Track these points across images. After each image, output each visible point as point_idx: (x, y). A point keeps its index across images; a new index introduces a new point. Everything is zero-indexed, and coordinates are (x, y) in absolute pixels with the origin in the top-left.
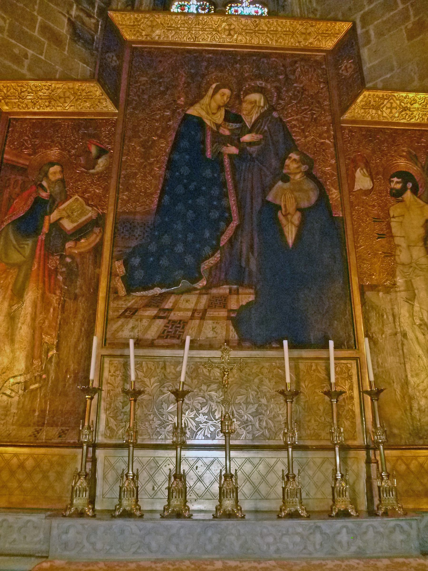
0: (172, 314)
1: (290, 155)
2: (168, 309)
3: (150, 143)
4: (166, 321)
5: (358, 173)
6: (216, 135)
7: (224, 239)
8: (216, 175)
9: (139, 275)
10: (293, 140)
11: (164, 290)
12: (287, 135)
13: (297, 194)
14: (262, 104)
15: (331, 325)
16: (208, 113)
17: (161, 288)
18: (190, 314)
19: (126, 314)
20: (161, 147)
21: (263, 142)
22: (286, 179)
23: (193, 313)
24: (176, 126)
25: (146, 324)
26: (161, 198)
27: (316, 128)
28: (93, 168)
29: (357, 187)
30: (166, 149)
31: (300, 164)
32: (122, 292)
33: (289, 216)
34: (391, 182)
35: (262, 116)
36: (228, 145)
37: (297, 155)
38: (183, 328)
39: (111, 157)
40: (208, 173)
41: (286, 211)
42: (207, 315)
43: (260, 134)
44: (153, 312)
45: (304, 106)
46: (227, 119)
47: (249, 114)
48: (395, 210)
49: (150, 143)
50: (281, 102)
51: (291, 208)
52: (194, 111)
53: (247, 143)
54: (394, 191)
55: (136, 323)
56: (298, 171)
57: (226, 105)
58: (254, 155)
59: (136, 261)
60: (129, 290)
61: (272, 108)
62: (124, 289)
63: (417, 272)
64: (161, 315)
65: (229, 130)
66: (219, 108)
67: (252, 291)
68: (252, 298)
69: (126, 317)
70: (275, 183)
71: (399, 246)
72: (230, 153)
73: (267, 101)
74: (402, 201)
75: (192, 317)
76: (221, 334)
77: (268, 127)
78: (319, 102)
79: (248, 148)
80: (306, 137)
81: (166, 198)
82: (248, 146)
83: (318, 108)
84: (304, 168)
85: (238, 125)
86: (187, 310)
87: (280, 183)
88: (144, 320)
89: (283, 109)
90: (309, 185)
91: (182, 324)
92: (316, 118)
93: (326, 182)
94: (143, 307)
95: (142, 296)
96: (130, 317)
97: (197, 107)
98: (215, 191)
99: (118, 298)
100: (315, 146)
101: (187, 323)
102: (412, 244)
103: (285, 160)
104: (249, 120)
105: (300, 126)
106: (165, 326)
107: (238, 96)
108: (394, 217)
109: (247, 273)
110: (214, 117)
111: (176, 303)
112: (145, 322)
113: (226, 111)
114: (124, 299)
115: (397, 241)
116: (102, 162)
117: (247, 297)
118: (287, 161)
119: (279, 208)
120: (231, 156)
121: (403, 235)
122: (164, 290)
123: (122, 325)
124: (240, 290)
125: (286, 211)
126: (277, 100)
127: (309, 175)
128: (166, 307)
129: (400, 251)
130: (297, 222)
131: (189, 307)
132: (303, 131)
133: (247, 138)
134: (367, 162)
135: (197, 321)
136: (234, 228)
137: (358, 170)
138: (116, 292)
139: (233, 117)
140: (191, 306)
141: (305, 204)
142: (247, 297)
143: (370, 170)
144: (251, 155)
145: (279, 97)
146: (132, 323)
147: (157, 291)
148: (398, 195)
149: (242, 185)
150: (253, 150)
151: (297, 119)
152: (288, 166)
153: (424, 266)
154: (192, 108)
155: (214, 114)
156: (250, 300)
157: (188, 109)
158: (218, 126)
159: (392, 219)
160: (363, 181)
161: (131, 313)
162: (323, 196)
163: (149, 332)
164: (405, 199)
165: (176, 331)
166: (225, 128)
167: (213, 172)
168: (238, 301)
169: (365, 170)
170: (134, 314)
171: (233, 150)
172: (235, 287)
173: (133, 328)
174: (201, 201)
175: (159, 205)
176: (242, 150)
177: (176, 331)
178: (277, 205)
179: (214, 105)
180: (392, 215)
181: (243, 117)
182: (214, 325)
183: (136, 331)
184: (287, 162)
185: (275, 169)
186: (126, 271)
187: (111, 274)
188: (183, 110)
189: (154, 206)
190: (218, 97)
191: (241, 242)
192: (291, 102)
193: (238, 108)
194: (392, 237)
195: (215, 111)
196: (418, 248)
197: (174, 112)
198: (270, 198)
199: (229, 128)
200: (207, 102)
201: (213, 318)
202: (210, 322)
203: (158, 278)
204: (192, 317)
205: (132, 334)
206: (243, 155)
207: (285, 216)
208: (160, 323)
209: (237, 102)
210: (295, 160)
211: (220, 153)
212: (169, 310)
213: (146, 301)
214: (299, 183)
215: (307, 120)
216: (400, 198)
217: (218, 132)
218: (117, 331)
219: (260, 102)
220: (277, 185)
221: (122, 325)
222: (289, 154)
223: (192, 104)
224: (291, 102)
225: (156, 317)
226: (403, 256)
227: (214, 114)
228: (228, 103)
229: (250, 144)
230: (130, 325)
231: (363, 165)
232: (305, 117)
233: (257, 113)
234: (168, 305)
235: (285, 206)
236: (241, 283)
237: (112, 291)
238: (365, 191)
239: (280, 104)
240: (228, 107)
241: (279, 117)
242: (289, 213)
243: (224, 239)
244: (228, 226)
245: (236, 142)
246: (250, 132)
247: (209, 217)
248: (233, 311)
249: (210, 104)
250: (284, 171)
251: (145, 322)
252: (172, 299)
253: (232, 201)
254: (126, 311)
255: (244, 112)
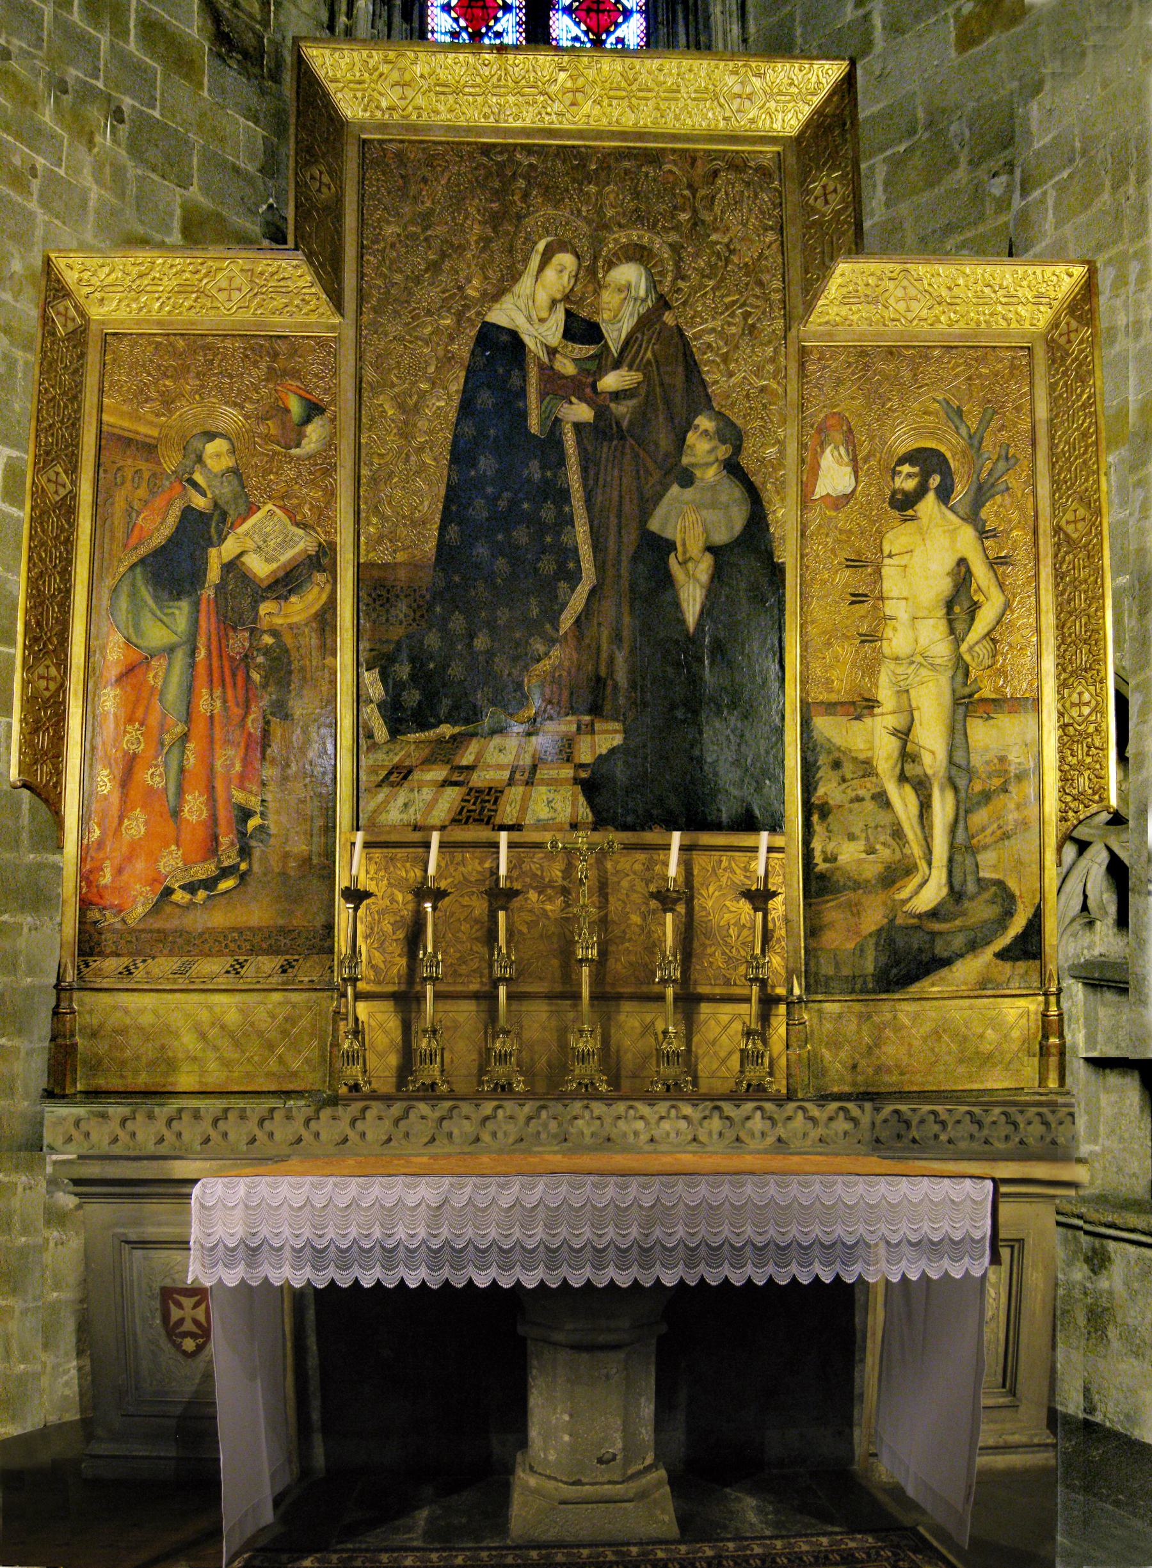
0: (475, 776)
1: (696, 422)
2: (467, 768)
3: (415, 397)
4: (464, 790)
5: (828, 459)
6: (549, 374)
7: (567, 620)
8: (549, 474)
9: (412, 697)
10: (703, 383)
11: (457, 730)
12: (692, 368)
13: (704, 513)
14: (642, 293)
15: (759, 789)
16: (529, 319)
17: (454, 724)
18: (506, 774)
19: (392, 778)
20: (438, 408)
21: (643, 392)
22: (687, 479)
23: (513, 773)
24: (466, 355)
25: (430, 797)
26: (442, 529)
27: (753, 351)
28: (298, 445)
29: (823, 488)
30: (447, 414)
31: (715, 442)
32: (381, 733)
33: (690, 565)
34: (894, 473)
35: (644, 323)
36: (573, 399)
37: (711, 420)
38: (495, 802)
39: (333, 420)
40: (534, 469)
41: (684, 553)
42: (538, 776)
43: (638, 370)
44: (439, 773)
45: (728, 295)
46: (569, 334)
47: (616, 319)
48: (897, 538)
49: (415, 397)
50: (681, 284)
51: (695, 547)
52: (504, 314)
53: (611, 393)
54: (899, 497)
55: (411, 795)
56: (712, 458)
57: (567, 298)
58: (625, 424)
59: (403, 671)
60: (395, 732)
61: (663, 304)
62: (384, 729)
63: (924, 672)
64: (455, 778)
65: (574, 360)
66: (554, 303)
67: (617, 726)
68: (618, 740)
69: (392, 785)
70: (666, 488)
71: (892, 618)
72: (575, 420)
73: (653, 284)
74: (913, 519)
75: (511, 782)
76: (564, 812)
77: (653, 352)
78: (760, 284)
79: (613, 405)
80: (731, 374)
81: (453, 530)
82: (611, 400)
83: (757, 297)
84: (724, 451)
85: (592, 350)
86: (500, 767)
87: (675, 489)
88: (425, 790)
89: (684, 303)
90: (732, 492)
91: (494, 794)
92: (753, 325)
93: (764, 484)
94: (423, 763)
95: (418, 743)
96: (399, 784)
97: (507, 302)
98: (548, 513)
99: (374, 747)
100: (747, 396)
101: (502, 792)
102: (921, 615)
103: (687, 432)
104: (616, 334)
105: (719, 349)
106: (463, 800)
107: (592, 271)
108: (890, 556)
109: (609, 690)
110: (543, 328)
111: (479, 756)
112: (427, 794)
113: (569, 314)
114: (385, 748)
115: (890, 608)
116: (315, 432)
117: (608, 738)
118: (690, 434)
119: (671, 546)
120: (578, 427)
121: (905, 594)
122: (457, 730)
123: (386, 801)
124: (597, 726)
125: (684, 553)
126: (675, 279)
127: (733, 468)
128: (464, 762)
129: (895, 629)
130: (704, 577)
131: (506, 761)
132: (725, 359)
133: (611, 381)
134: (850, 430)
135: (521, 789)
136: (585, 595)
137: (828, 451)
138: (370, 736)
139: (582, 329)
140: (507, 759)
141: (721, 537)
142: (608, 738)
143: (854, 451)
144: (618, 424)
145: (680, 276)
146: (402, 796)
147: (446, 730)
148: (904, 503)
149: (600, 499)
150: (622, 410)
151: (713, 330)
152: (691, 447)
153: (938, 661)
154: (497, 306)
155: (542, 321)
156: (615, 743)
157: (490, 309)
158: (552, 352)
159: (887, 561)
160: (835, 475)
161: (400, 775)
162: (757, 519)
163: (434, 813)
164: (919, 514)
165: (483, 808)
166: (566, 357)
167: (543, 468)
168: (593, 747)
169: (842, 450)
170: (405, 778)
171: (583, 412)
172: (587, 718)
173: (406, 805)
174: (521, 535)
175: (441, 545)
176: (601, 413)
177: (483, 808)
178: (667, 540)
179: (543, 298)
180: (886, 553)
181: (603, 326)
182: (551, 796)
183: (412, 811)
184: (691, 437)
185: (667, 455)
186: (386, 691)
187: (359, 699)
188: (478, 314)
189: (430, 546)
190: (550, 273)
191: (599, 624)
192: (702, 286)
193: (592, 305)
194: (882, 598)
195: (544, 315)
196: (931, 621)
197: (460, 316)
198: (654, 525)
199: (574, 356)
200: (528, 292)
201: (549, 782)
202: (543, 789)
203: (445, 704)
204: (511, 782)
205: (405, 817)
206: (603, 429)
207: (683, 564)
208: (452, 795)
209: (590, 288)
210: (706, 432)
211: (557, 421)
212: (471, 768)
213: (427, 751)
214: (713, 487)
215: (733, 330)
216: (910, 512)
217: (552, 368)
218: (377, 811)
219: (638, 287)
220: (668, 494)
221: (386, 801)
222: (695, 417)
223: (497, 297)
224: (702, 286)
225: (446, 783)
226: (897, 641)
227: (542, 321)
228: (572, 290)
229: (616, 396)
230: (401, 801)
231: (838, 437)
232: (729, 324)
233: (632, 315)
234: (467, 759)
235: (684, 540)
236: (596, 710)
237: (362, 732)
238: (838, 498)
239: (679, 290)
240: (572, 302)
241: (677, 326)
242: (690, 558)
243: (567, 620)
244: (573, 590)
245: (588, 390)
246: (617, 365)
247: (536, 570)
248: (582, 766)
249: (533, 297)
250: (685, 460)
251: (427, 794)
252: (474, 746)
253: (581, 533)
254: (390, 773)
255: (606, 315)
